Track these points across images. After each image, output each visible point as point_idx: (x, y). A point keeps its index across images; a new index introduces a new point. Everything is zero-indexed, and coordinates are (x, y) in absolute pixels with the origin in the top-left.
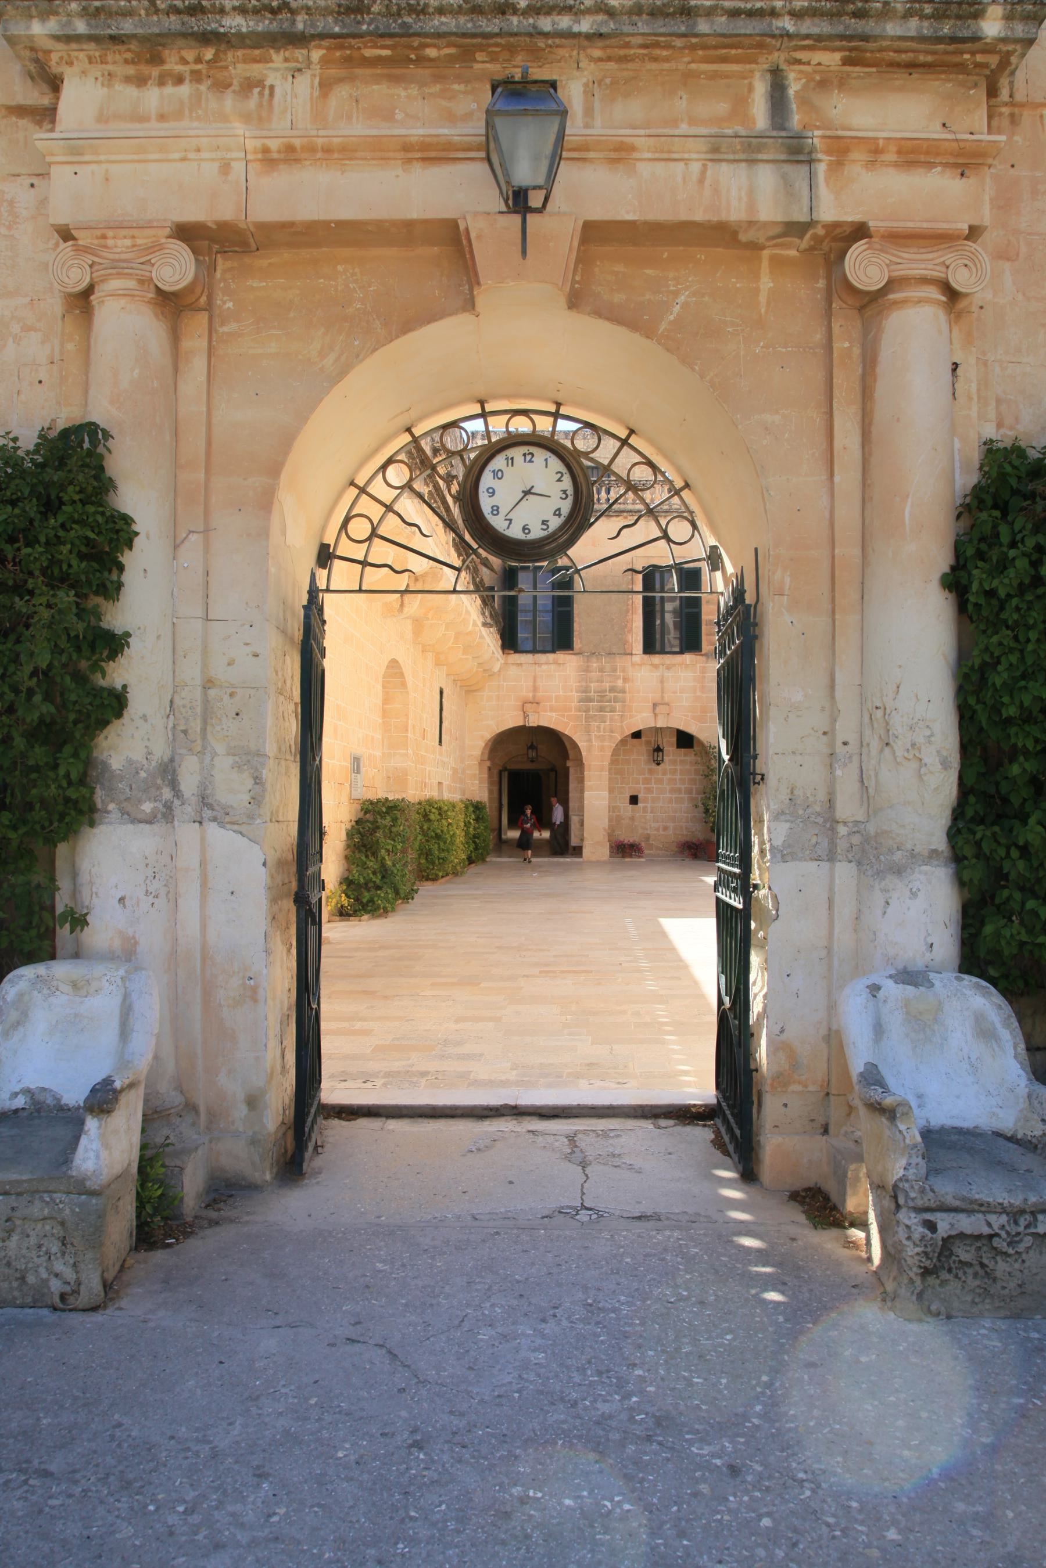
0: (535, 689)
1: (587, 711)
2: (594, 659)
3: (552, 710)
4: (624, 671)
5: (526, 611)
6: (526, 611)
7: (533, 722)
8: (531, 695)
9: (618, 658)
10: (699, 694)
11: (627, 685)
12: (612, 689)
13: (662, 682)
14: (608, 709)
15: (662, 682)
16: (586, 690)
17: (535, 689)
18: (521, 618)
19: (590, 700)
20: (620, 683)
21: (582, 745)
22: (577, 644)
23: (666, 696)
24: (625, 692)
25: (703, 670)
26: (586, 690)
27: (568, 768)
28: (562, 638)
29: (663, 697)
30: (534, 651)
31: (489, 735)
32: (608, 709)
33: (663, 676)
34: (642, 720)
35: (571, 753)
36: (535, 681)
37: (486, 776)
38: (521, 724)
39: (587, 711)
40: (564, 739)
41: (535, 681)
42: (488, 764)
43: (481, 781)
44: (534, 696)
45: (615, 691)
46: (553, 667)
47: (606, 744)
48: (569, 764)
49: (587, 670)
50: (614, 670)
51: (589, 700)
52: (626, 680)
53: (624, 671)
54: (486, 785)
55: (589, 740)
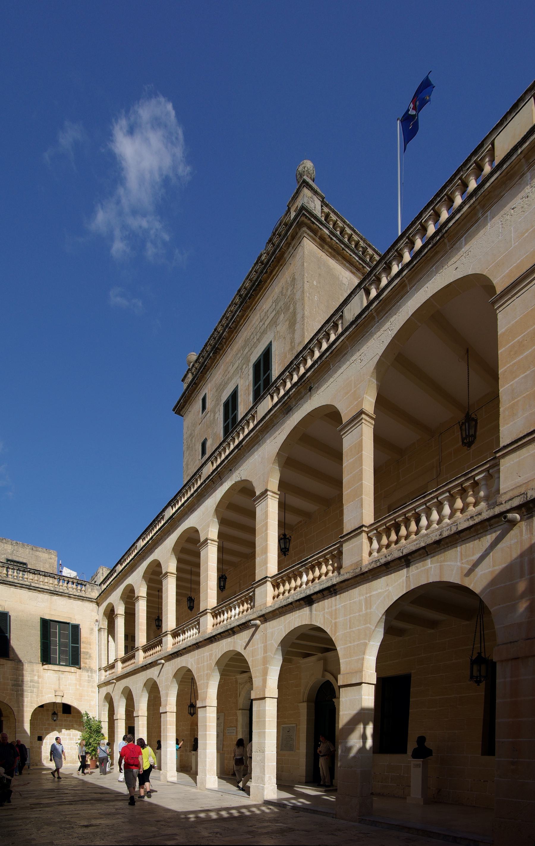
4: (38, 672)
9: (35, 665)
10: (78, 687)
11: (40, 680)
13: (59, 680)
15: (59, 680)
20: (36, 678)
23: (61, 687)
24: (39, 683)
25: (80, 676)
29: (59, 687)
33: (59, 677)
34: (48, 698)
45: (33, 682)
50: (33, 671)
52: (39, 677)
53: (38, 672)
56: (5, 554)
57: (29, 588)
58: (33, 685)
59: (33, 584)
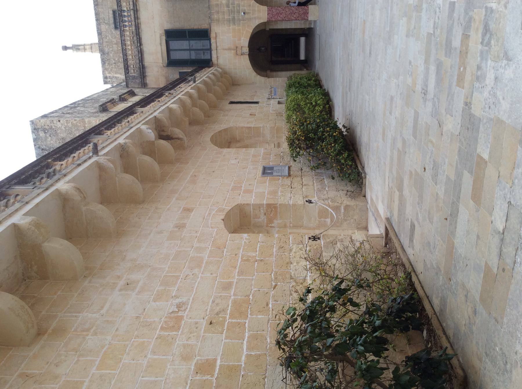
0: (229, 49)
1: (239, 20)
2: (213, 17)
3: (240, 40)
5: (190, 54)
6: (190, 54)
7: (246, 50)
8: (233, 51)
12: (228, 6)
14: (238, 8)
16: (229, 21)
17: (229, 49)
18: (193, 57)
19: (234, 19)
21: (257, 22)
22: (205, 26)
26: (229, 21)
27: (270, 29)
28: (203, 34)
30: (210, 50)
31: (254, 74)
32: (238, 8)
35: (262, 28)
36: (226, 49)
37: (274, 73)
38: (247, 57)
39: (239, 20)
40: (255, 32)
41: (226, 49)
42: (268, 72)
43: (276, 77)
44: (233, 50)
46: (218, 40)
47: (256, 9)
48: (268, 29)
49: (218, 20)
51: (234, 19)
54: (280, 73)
55: (255, 18)
56: (111, 31)
57: (136, 11)
58: (232, 4)
59: (131, 8)
